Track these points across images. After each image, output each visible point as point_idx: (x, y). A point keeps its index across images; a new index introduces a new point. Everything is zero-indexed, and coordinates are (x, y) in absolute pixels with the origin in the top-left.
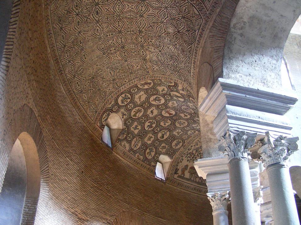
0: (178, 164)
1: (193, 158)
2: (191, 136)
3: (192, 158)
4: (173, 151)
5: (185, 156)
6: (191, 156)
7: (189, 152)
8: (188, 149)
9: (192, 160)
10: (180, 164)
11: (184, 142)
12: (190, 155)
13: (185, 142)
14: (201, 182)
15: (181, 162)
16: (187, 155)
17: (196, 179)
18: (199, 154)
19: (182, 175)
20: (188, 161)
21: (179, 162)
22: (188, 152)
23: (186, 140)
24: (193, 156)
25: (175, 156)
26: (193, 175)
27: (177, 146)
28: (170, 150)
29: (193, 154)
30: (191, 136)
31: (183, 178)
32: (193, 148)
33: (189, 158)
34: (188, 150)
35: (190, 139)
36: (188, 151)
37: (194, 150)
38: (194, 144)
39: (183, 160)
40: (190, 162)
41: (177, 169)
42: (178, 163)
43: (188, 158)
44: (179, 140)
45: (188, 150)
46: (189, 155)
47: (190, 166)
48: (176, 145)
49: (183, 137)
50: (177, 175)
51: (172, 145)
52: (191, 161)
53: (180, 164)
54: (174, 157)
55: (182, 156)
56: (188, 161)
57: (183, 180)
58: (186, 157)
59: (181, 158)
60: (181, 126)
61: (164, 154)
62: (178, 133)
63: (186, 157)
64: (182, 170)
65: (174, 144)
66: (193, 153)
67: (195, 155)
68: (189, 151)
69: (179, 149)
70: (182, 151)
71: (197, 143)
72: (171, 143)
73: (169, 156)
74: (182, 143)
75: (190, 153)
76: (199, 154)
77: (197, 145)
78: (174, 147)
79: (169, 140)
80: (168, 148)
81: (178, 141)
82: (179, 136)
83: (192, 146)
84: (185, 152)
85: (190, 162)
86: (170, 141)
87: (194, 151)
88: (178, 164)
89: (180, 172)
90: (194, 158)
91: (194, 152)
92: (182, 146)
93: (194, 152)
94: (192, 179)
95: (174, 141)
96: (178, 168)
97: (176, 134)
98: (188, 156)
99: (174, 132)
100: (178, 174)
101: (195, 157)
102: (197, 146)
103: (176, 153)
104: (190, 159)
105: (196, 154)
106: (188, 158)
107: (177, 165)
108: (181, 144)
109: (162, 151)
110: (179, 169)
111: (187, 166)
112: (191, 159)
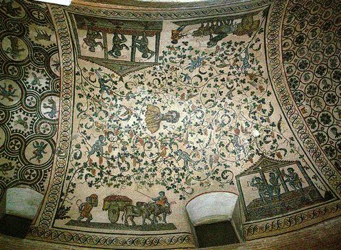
0: (63, 198)
1: (101, 174)
2: (58, 120)
3: (97, 177)
4: (37, 170)
5: (77, 175)
6: (94, 172)
7: (81, 161)
8: (72, 155)
9: (102, 181)
10: (70, 195)
11: (53, 144)
12: (89, 170)
13: (54, 141)
14: (153, 223)
15: (72, 191)
16: (82, 171)
17: (132, 220)
18: (111, 162)
19: (85, 219)
20: (90, 185)
21: (64, 191)
22: (77, 164)
23: (53, 134)
24: (98, 171)
25: (48, 179)
26: (121, 213)
27: (42, 156)
28: (29, 171)
29: (95, 165)
30: (58, 120)
31: (88, 224)
32: (83, 149)
33: (90, 179)
34: (75, 157)
35: (61, 128)
36: (75, 161)
37: (91, 153)
38: (79, 140)
39: (74, 185)
40: (98, 187)
41: (63, 208)
42: (62, 194)
43: (86, 178)
44: (39, 141)
45: (75, 157)
46: (86, 172)
47: (105, 196)
48: (39, 154)
49: (42, 131)
50: (67, 220)
51: (28, 159)
52: (99, 184)
53: (70, 195)
54: (45, 184)
55: (68, 178)
56: (90, 185)
57: (88, 229)
58: (80, 177)
59: (67, 182)
60: (15, 102)
61: (16, 184)
62: (23, 123)
63: (80, 177)
64: (80, 209)
65: (29, 152)
66: (94, 162)
67: (102, 167)
68: (79, 161)
69: (51, 161)
70: (61, 165)
71: (84, 133)
72: (21, 153)
73: (30, 185)
74: (49, 146)
75: (85, 165)
76: (111, 162)
77: (89, 138)
78: (34, 161)
79: (14, 148)
80: (17, 166)
81: (37, 143)
82: (29, 130)
83: (78, 147)
84: (70, 167)
85: (98, 187)
86: (17, 148)
87: (91, 157)
88: (63, 198)
89: (74, 214)
90: (105, 176)
91: (95, 159)
92: (54, 152)
93: (95, 159)
94: (120, 221)
95: (26, 146)
96: (66, 205)
97: (20, 127)
98: (84, 174)
99: (12, 124)
100: (68, 217)
101: (104, 171)
102: (92, 142)
103: (49, 174)
104: (94, 179)
105: (105, 164)
106: (86, 178)
107: (61, 200)
108: (48, 149)
109: (3, 176)
110: (68, 209)
111: (93, 200)
112: (97, 180)
